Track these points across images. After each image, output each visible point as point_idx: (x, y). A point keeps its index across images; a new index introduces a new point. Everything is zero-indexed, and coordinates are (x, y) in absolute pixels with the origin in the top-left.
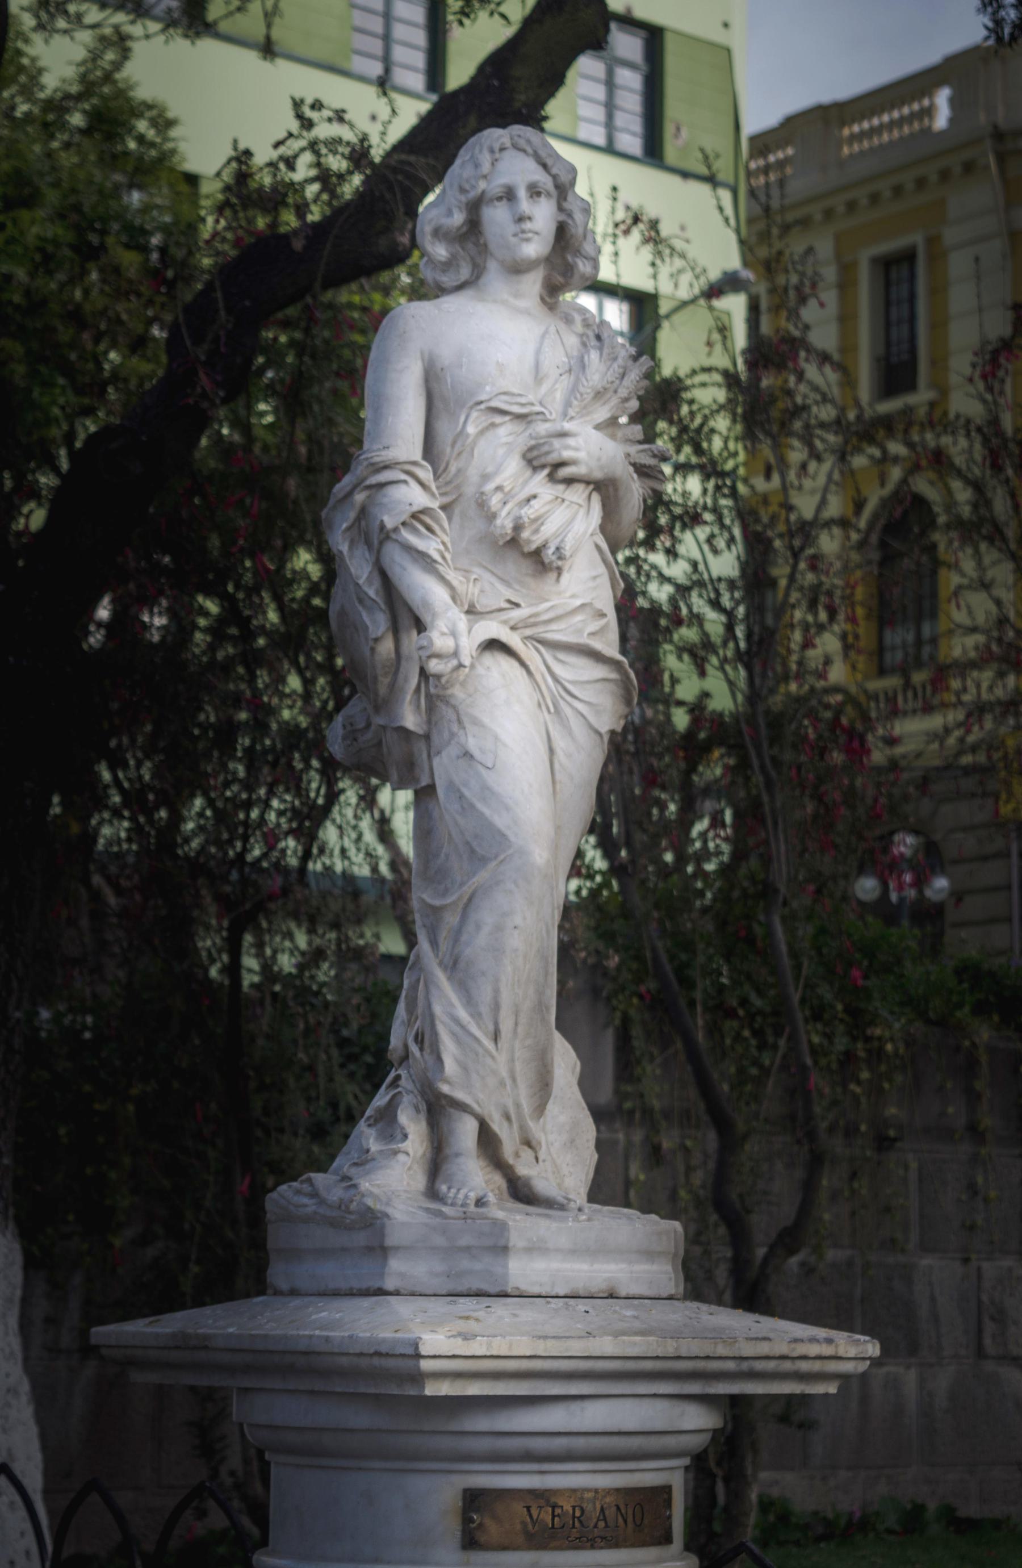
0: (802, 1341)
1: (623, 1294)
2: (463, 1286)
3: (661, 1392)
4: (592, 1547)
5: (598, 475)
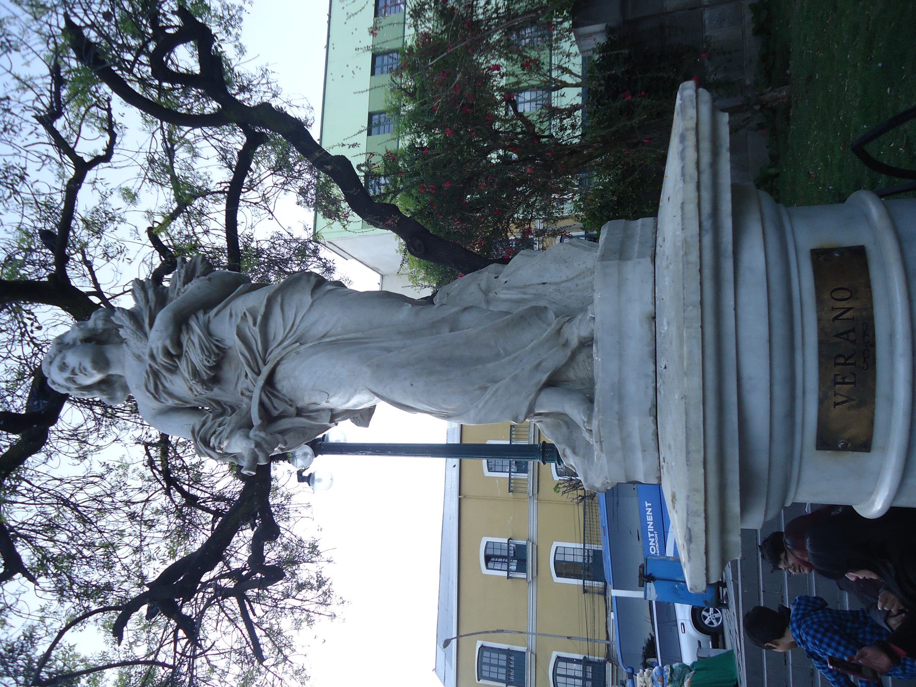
0: (683, 168)
1: (652, 307)
2: (653, 444)
3: (732, 303)
4: (873, 345)
5: (171, 328)
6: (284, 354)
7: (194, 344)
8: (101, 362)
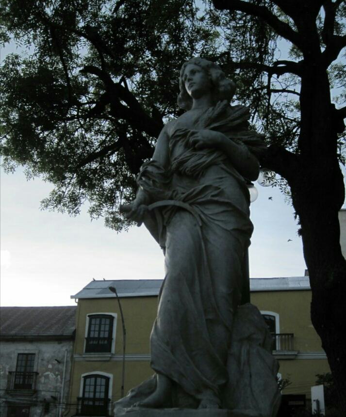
6: (196, 216)
7: (199, 159)
8: (197, 94)
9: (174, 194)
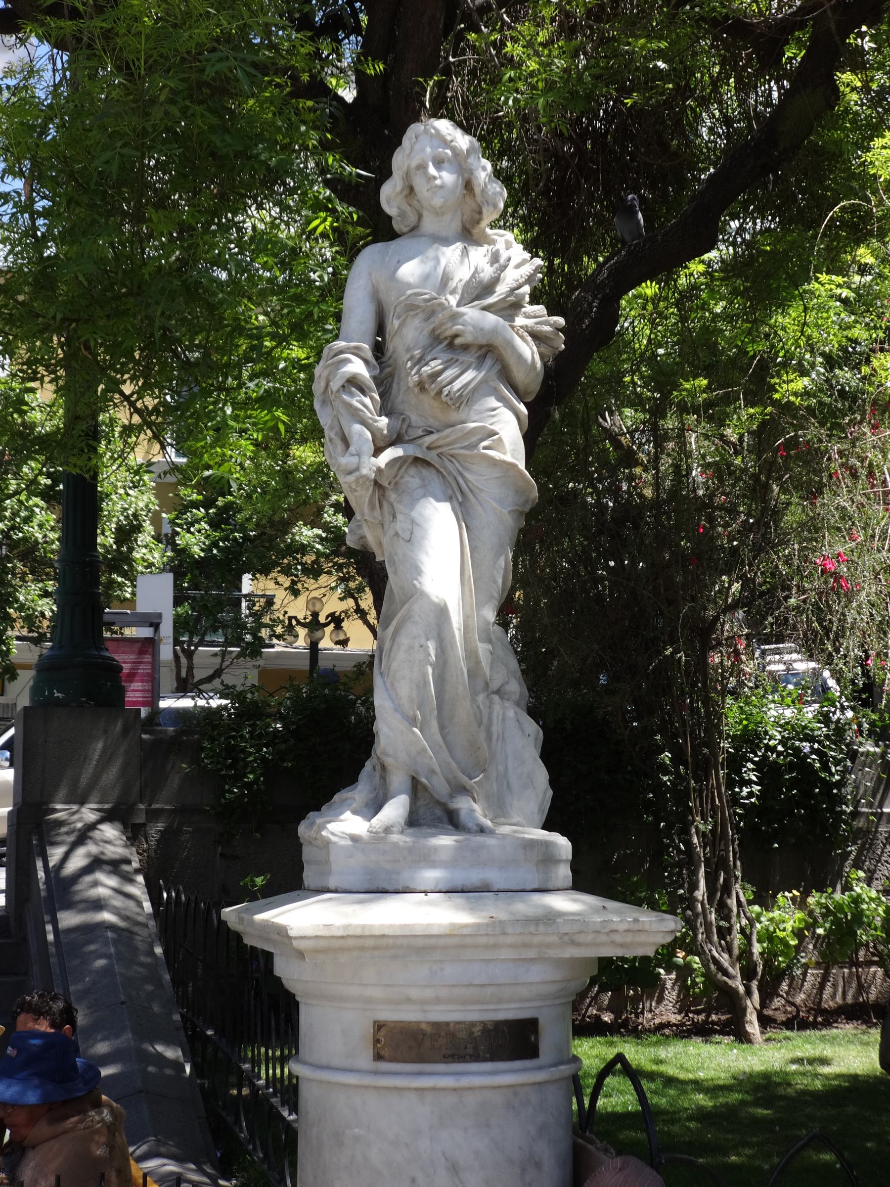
2: (373, 888)
5: (483, 341)
9: (405, 427)
